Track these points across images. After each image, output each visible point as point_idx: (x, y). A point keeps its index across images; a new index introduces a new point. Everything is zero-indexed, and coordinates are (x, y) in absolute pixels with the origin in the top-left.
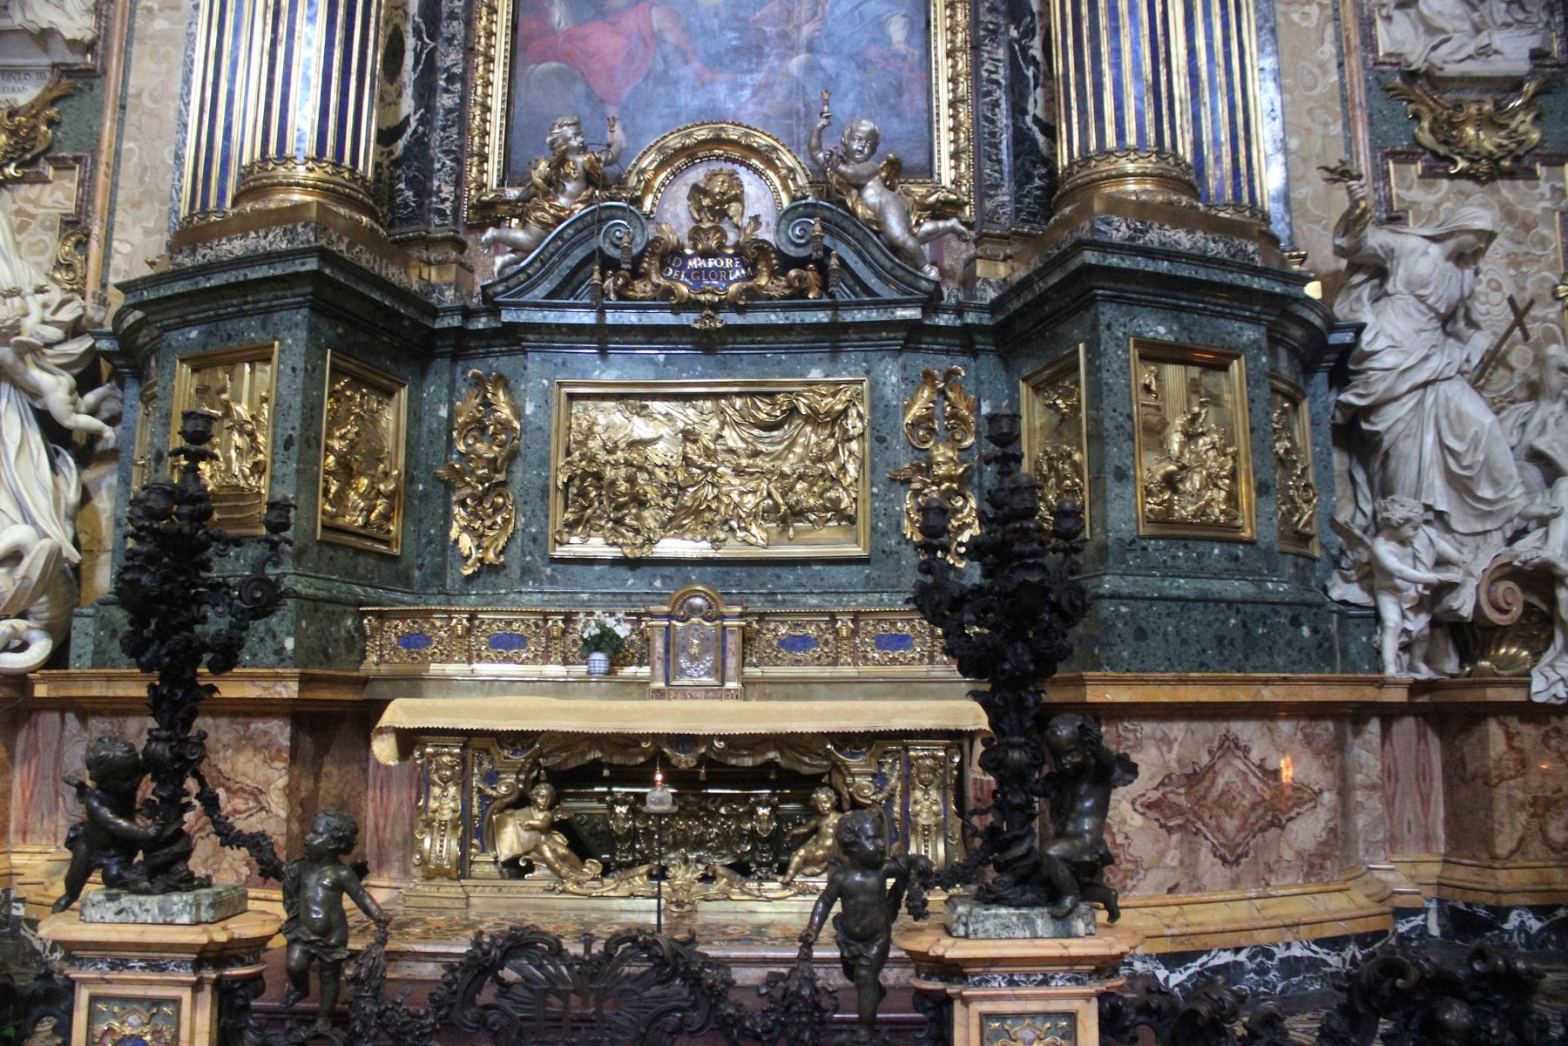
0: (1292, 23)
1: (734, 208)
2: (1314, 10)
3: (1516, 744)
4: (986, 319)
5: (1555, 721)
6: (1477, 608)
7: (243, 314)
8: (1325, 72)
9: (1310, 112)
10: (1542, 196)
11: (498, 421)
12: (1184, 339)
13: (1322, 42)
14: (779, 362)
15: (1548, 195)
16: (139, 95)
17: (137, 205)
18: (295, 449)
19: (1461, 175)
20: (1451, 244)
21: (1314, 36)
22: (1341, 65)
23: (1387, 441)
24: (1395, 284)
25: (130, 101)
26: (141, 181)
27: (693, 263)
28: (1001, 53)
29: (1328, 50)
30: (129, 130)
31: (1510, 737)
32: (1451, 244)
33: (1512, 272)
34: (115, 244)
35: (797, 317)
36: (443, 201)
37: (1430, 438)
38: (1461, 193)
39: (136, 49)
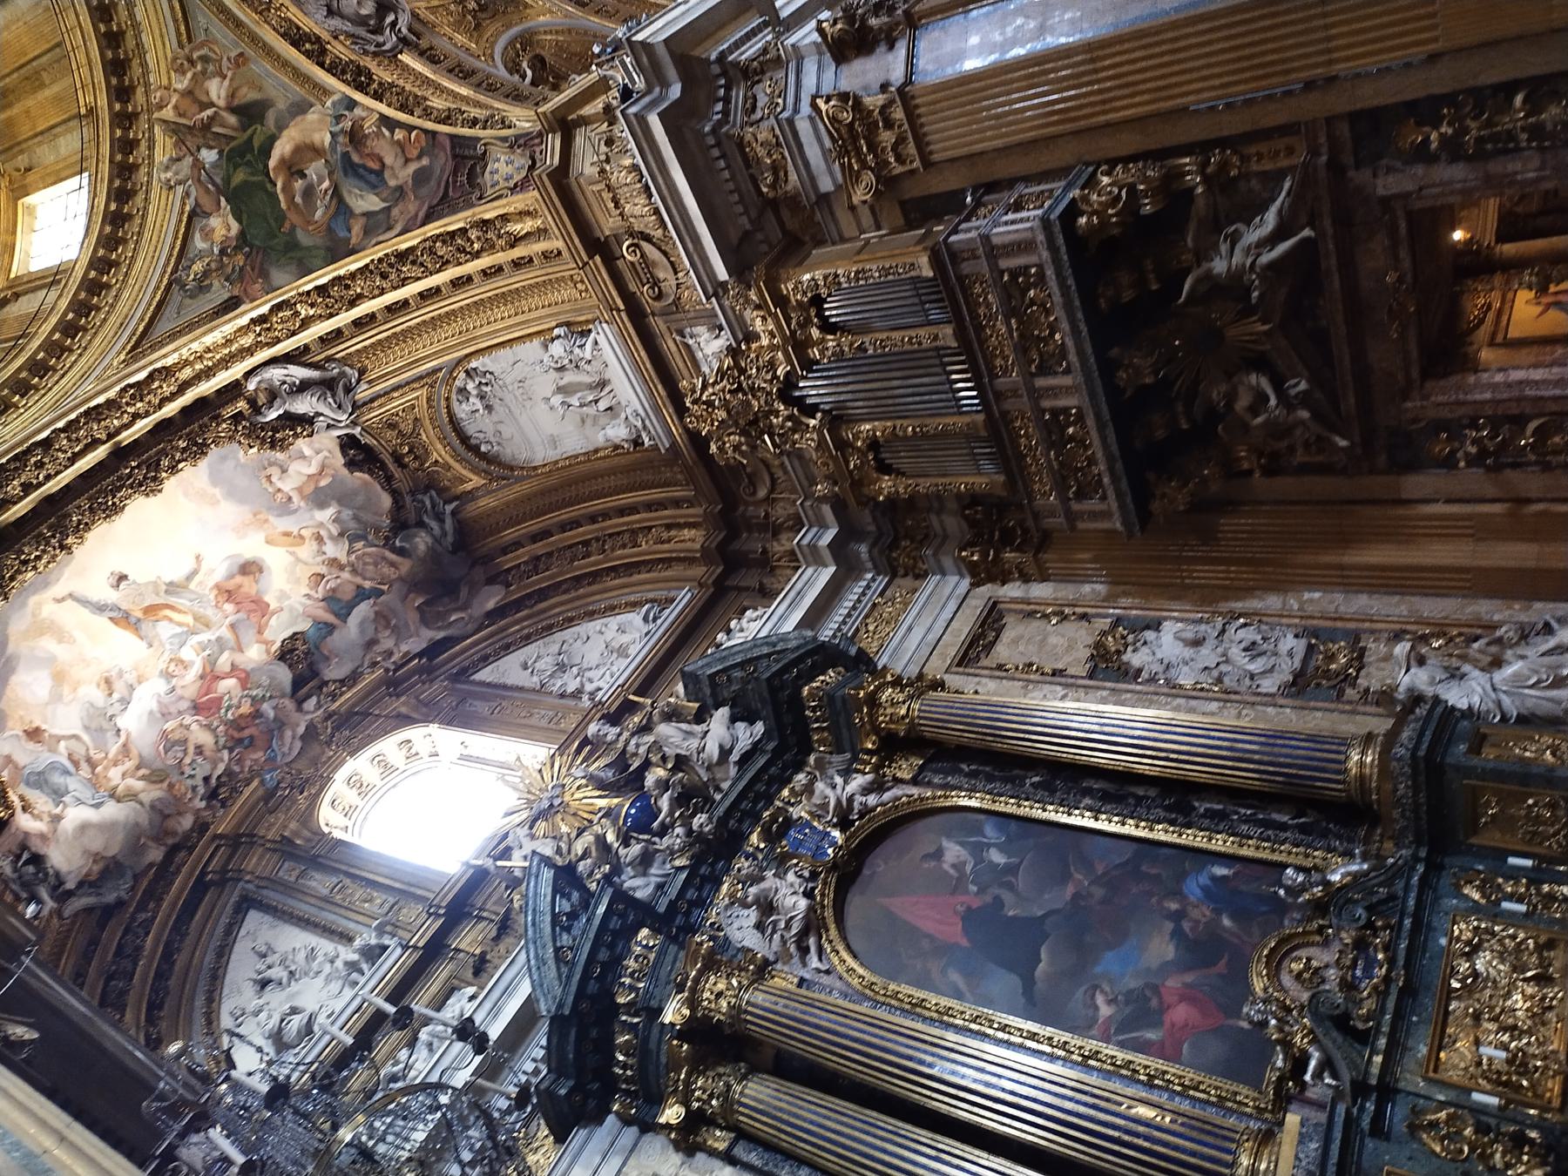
1: (1315, 963)
11: (1447, 1122)
14: (1431, 958)
20: (1413, 662)
23: (1525, 712)
27: (1358, 973)
29: (1270, 709)
32: (1413, 662)
35: (1405, 934)
37: (1527, 691)
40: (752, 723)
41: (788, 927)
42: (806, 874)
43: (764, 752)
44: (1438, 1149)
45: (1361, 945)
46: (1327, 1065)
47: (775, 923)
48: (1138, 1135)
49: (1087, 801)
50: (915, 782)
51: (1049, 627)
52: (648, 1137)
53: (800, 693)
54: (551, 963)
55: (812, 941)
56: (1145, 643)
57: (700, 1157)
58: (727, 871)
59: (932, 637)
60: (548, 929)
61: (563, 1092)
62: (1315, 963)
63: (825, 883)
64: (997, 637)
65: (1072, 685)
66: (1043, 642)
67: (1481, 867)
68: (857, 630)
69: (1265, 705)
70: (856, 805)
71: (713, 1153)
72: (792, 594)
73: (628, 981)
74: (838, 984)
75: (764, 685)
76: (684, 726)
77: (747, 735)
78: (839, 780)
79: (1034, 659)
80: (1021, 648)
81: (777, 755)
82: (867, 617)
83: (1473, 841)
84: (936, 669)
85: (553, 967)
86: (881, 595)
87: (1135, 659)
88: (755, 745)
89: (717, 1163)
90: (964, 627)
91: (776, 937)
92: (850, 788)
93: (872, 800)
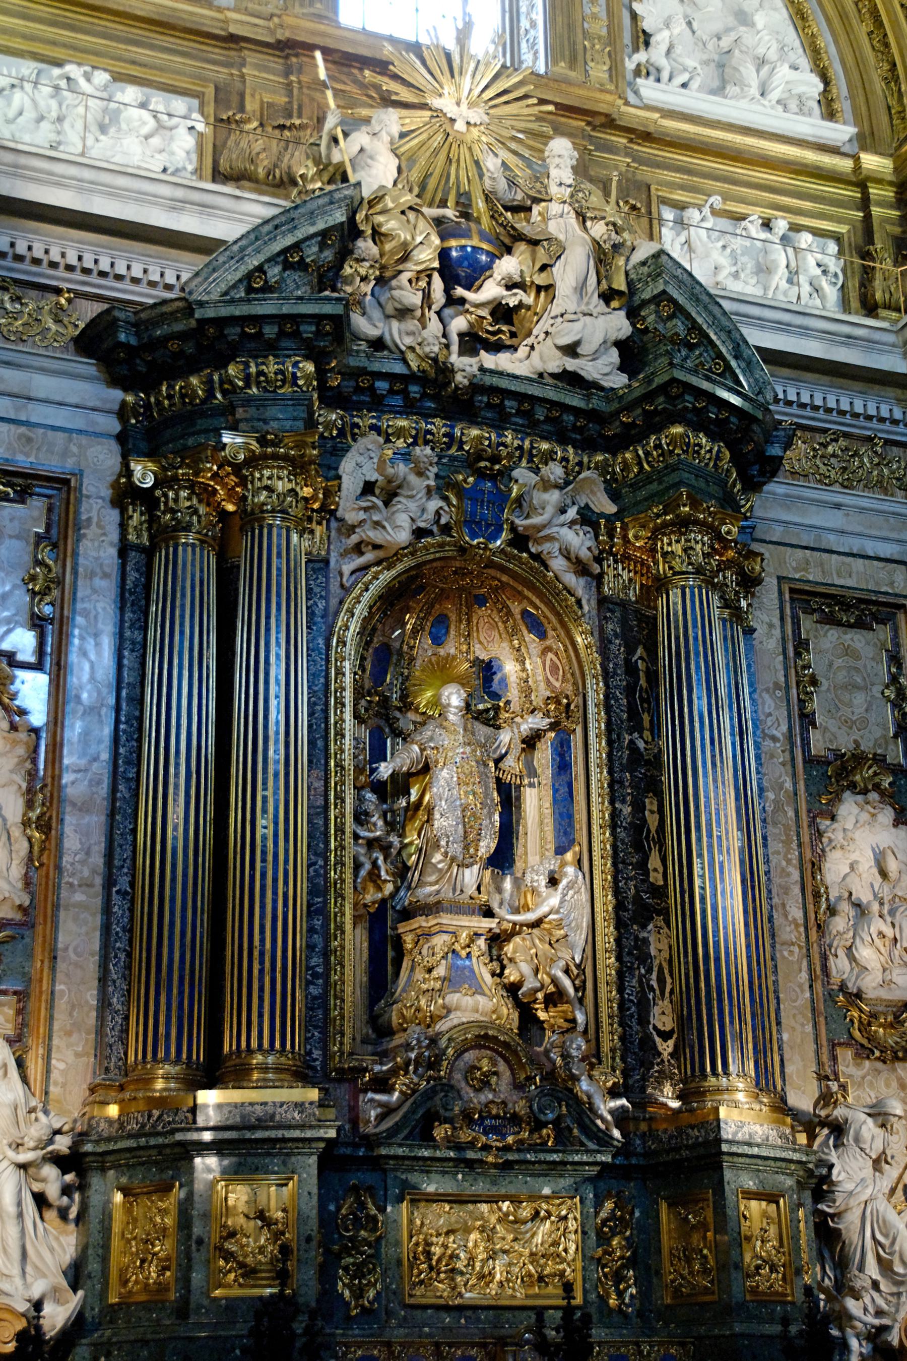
0: (784, 957)
1: (494, 1079)
2: (796, 949)
4: (642, 1162)
6: (901, 1340)
7: (269, 1154)
8: (802, 991)
9: (794, 1016)
11: (368, 1216)
12: (761, 1190)
16: (66, 949)
17: (69, 1034)
18: (314, 1243)
19: (878, 1059)
21: (796, 966)
22: (811, 986)
24: (849, 1140)
25: (60, 954)
26: (71, 1014)
28: (634, 982)
29: (804, 975)
30: (59, 976)
34: (54, 1062)
35: (542, 1156)
36: (315, 1060)
39: (62, 914)
40: (622, 368)
41: (377, 524)
42: (443, 521)
43: (588, 397)
44: (343, 1211)
45: (515, 1119)
46: (388, 1111)
47: (374, 507)
48: (262, 962)
49: (627, 810)
50: (603, 601)
51: (876, 690)
52: (115, 447)
53: (673, 423)
54: (243, 270)
55: (369, 556)
56: (873, 815)
57: (114, 515)
58: (427, 416)
59: (832, 541)
60: (277, 246)
61: (122, 337)
62: (494, 1079)
63: (442, 545)
64: (851, 626)
65: (792, 744)
66: (856, 687)
67: (637, 1214)
68: (825, 431)
69: (810, 969)
70: (546, 547)
71: (123, 526)
72: (846, 329)
73: (253, 370)
74: (334, 602)
75: (666, 378)
76: (593, 279)
77: (603, 369)
78: (572, 513)
79: (825, 684)
80: (838, 662)
81: (592, 415)
82: (846, 435)
83: (664, 1206)
84: (775, 565)
85: (239, 275)
86: (888, 442)
87: (850, 809)
88: (595, 385)
89: (115, 536)
90: (855, 577)
91: (362, 515)
92: (565, 531)
93: (558, 564)
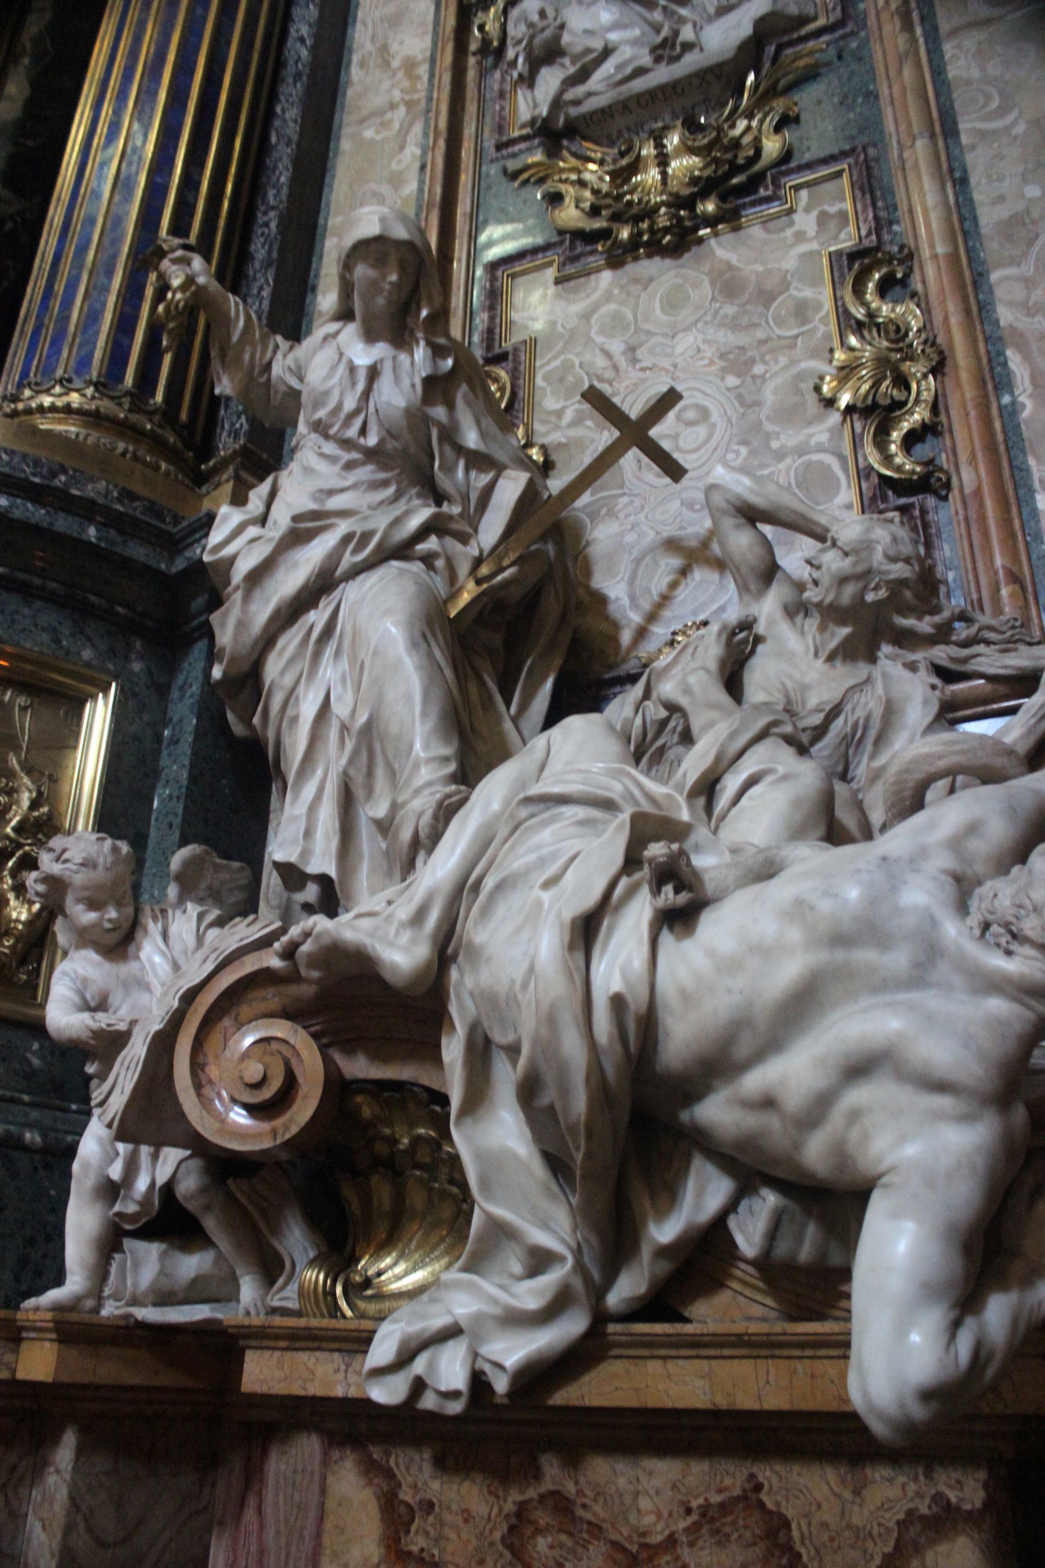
3: (415, 1542)
5: (553, 1473)
10: (800, 237)
13: (402, 148)
15: (811, 230)
22: (423, 167)
29: (412, 151)
31: (397, 1517)
33: (732, 381)
38: (636, 281)
